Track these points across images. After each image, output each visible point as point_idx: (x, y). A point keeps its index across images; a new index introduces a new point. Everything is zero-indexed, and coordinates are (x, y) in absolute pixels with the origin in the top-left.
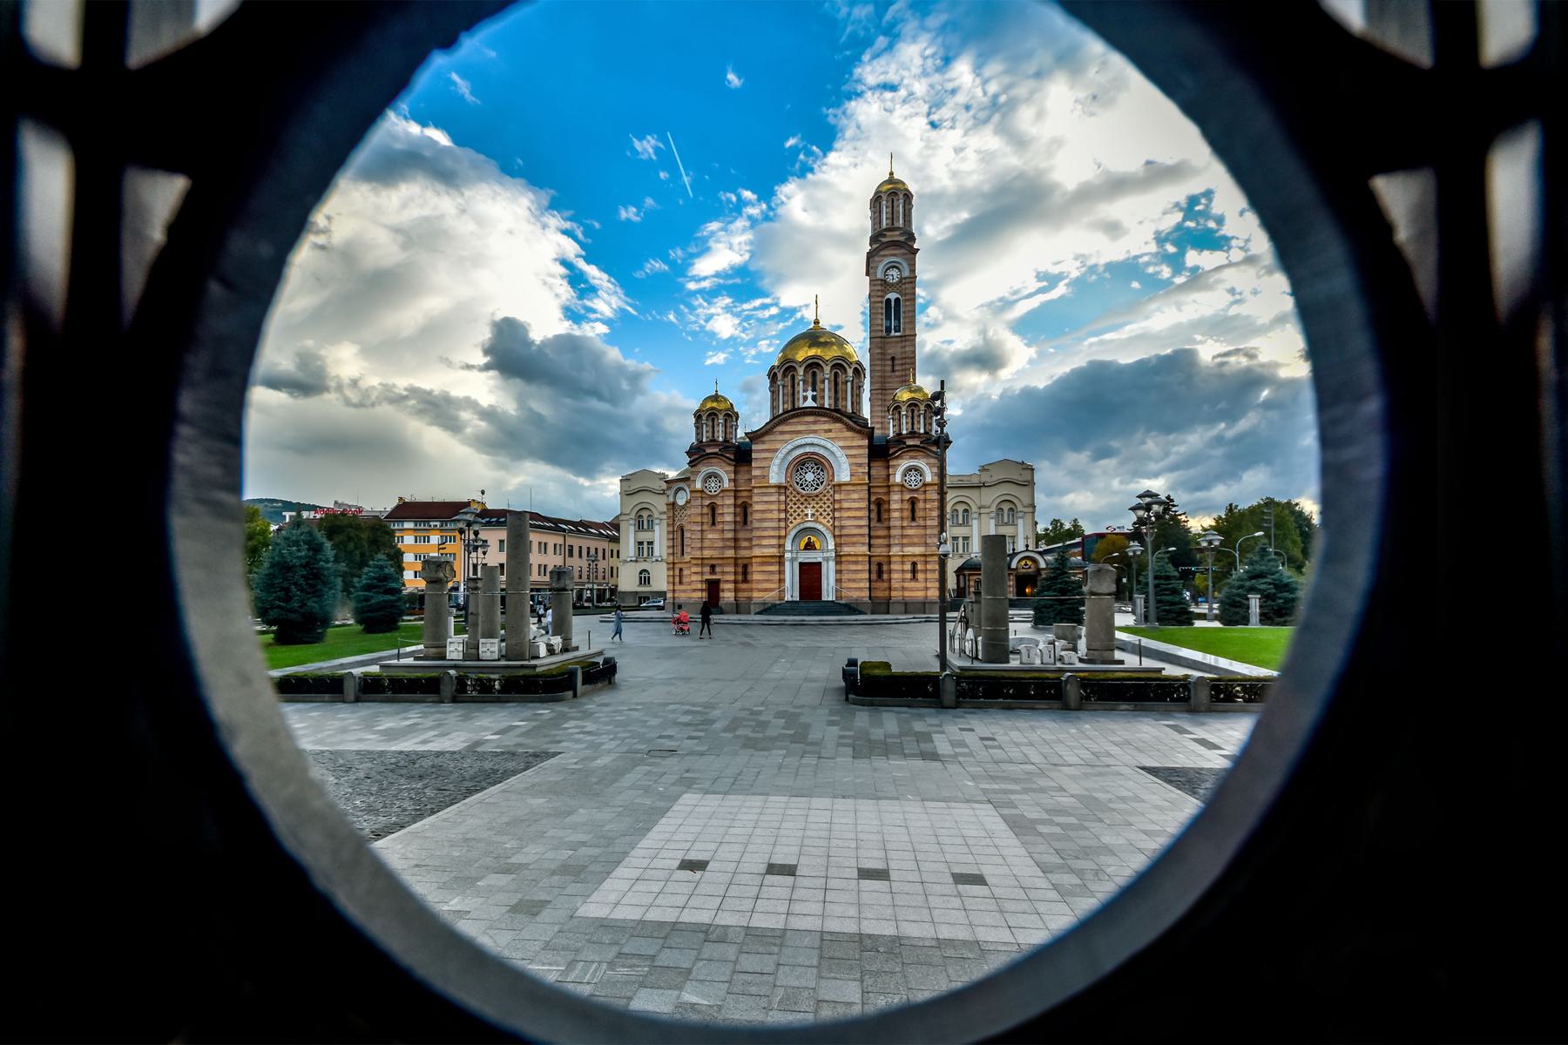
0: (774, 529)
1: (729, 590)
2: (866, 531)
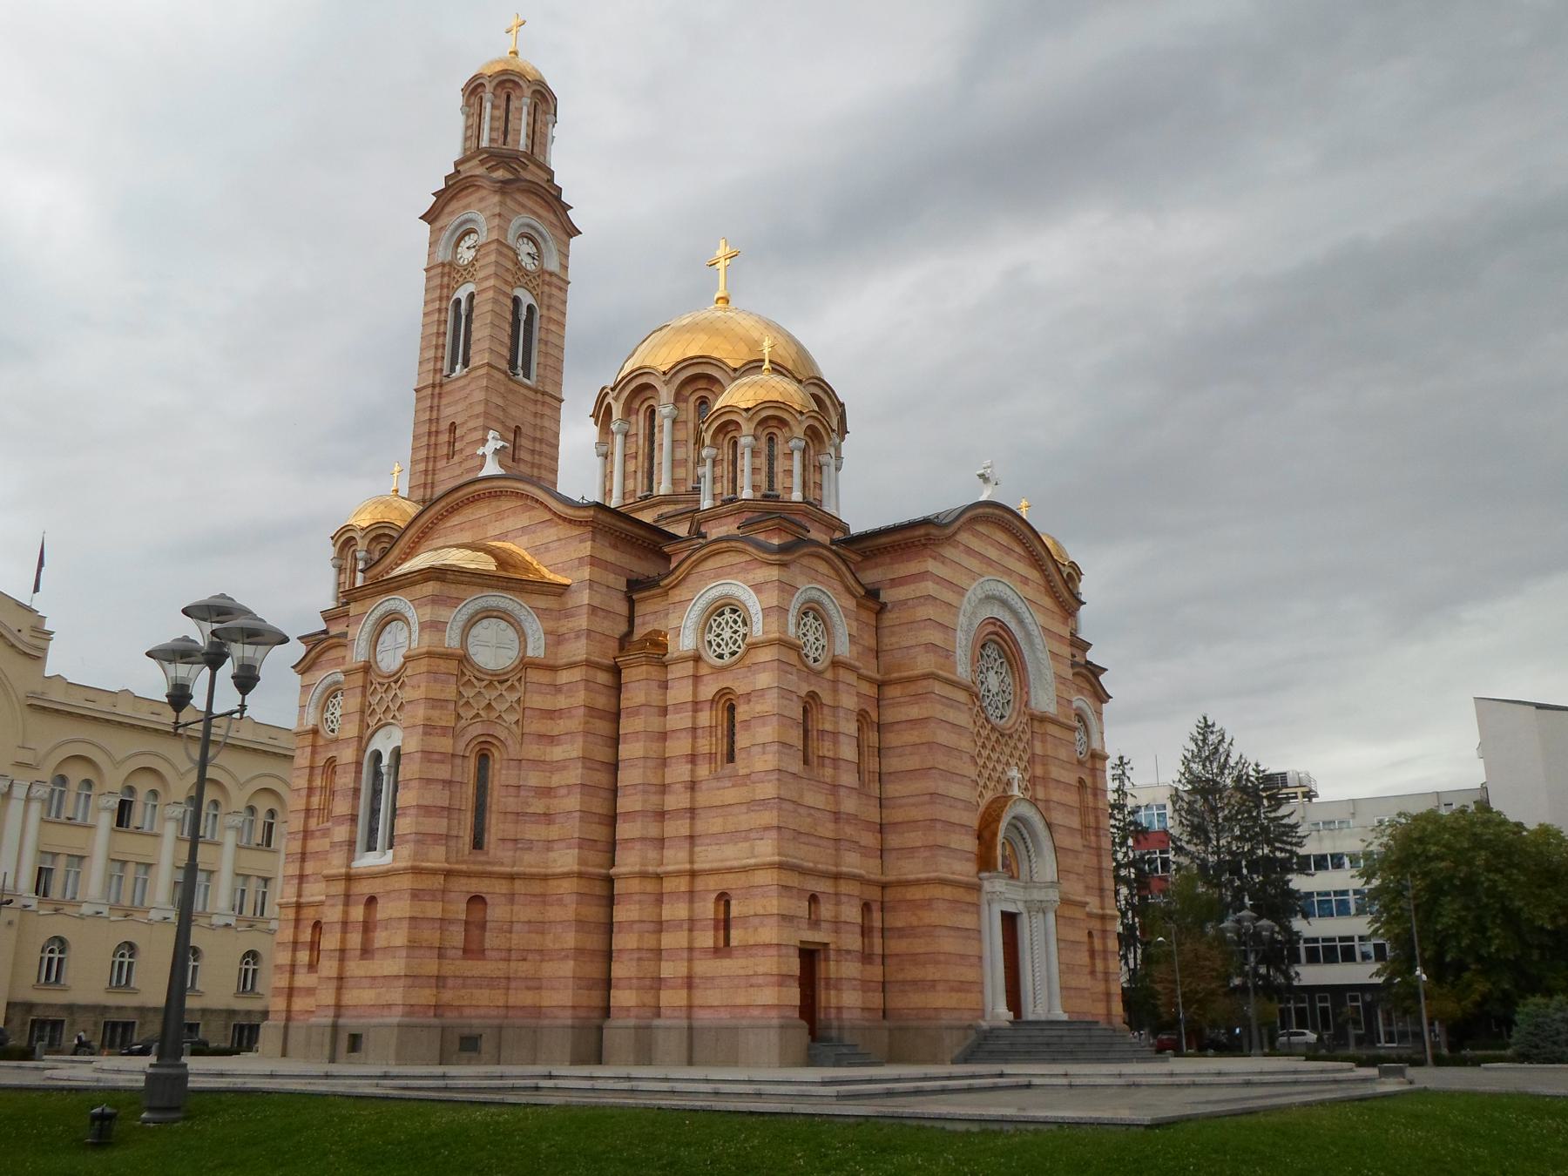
0: (969, 806)
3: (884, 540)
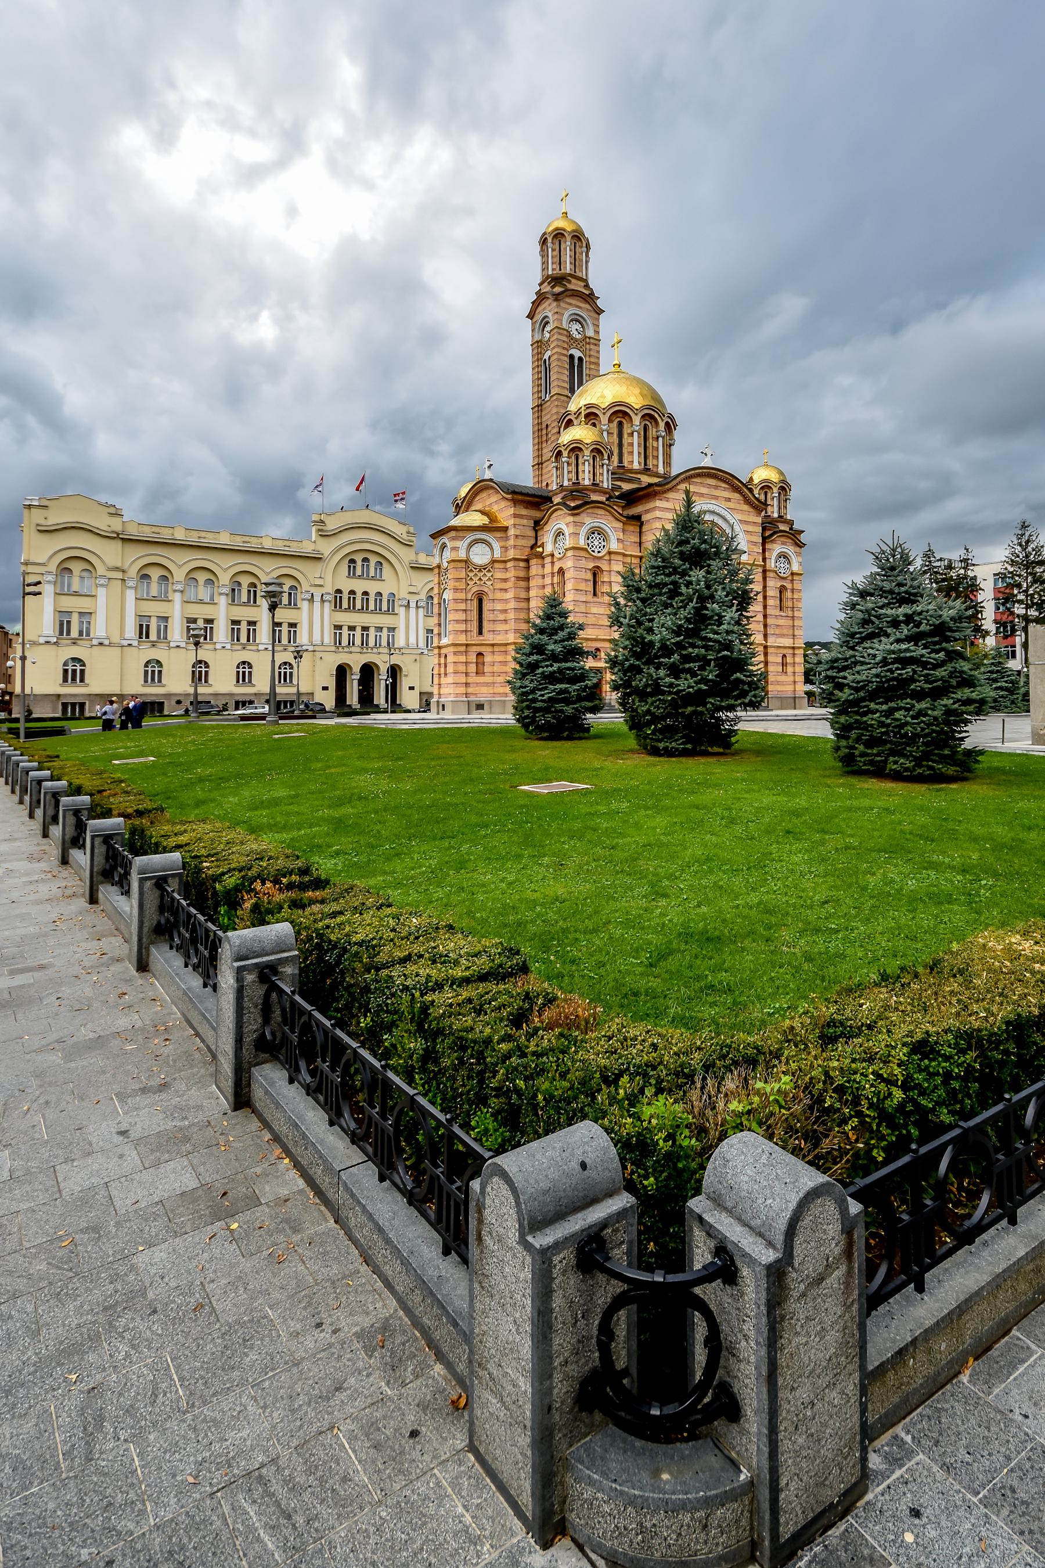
3: (641, 493)
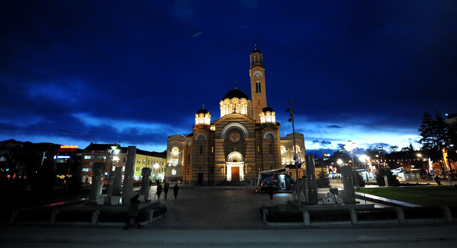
1: (206, 177)
2: (254, 156)
